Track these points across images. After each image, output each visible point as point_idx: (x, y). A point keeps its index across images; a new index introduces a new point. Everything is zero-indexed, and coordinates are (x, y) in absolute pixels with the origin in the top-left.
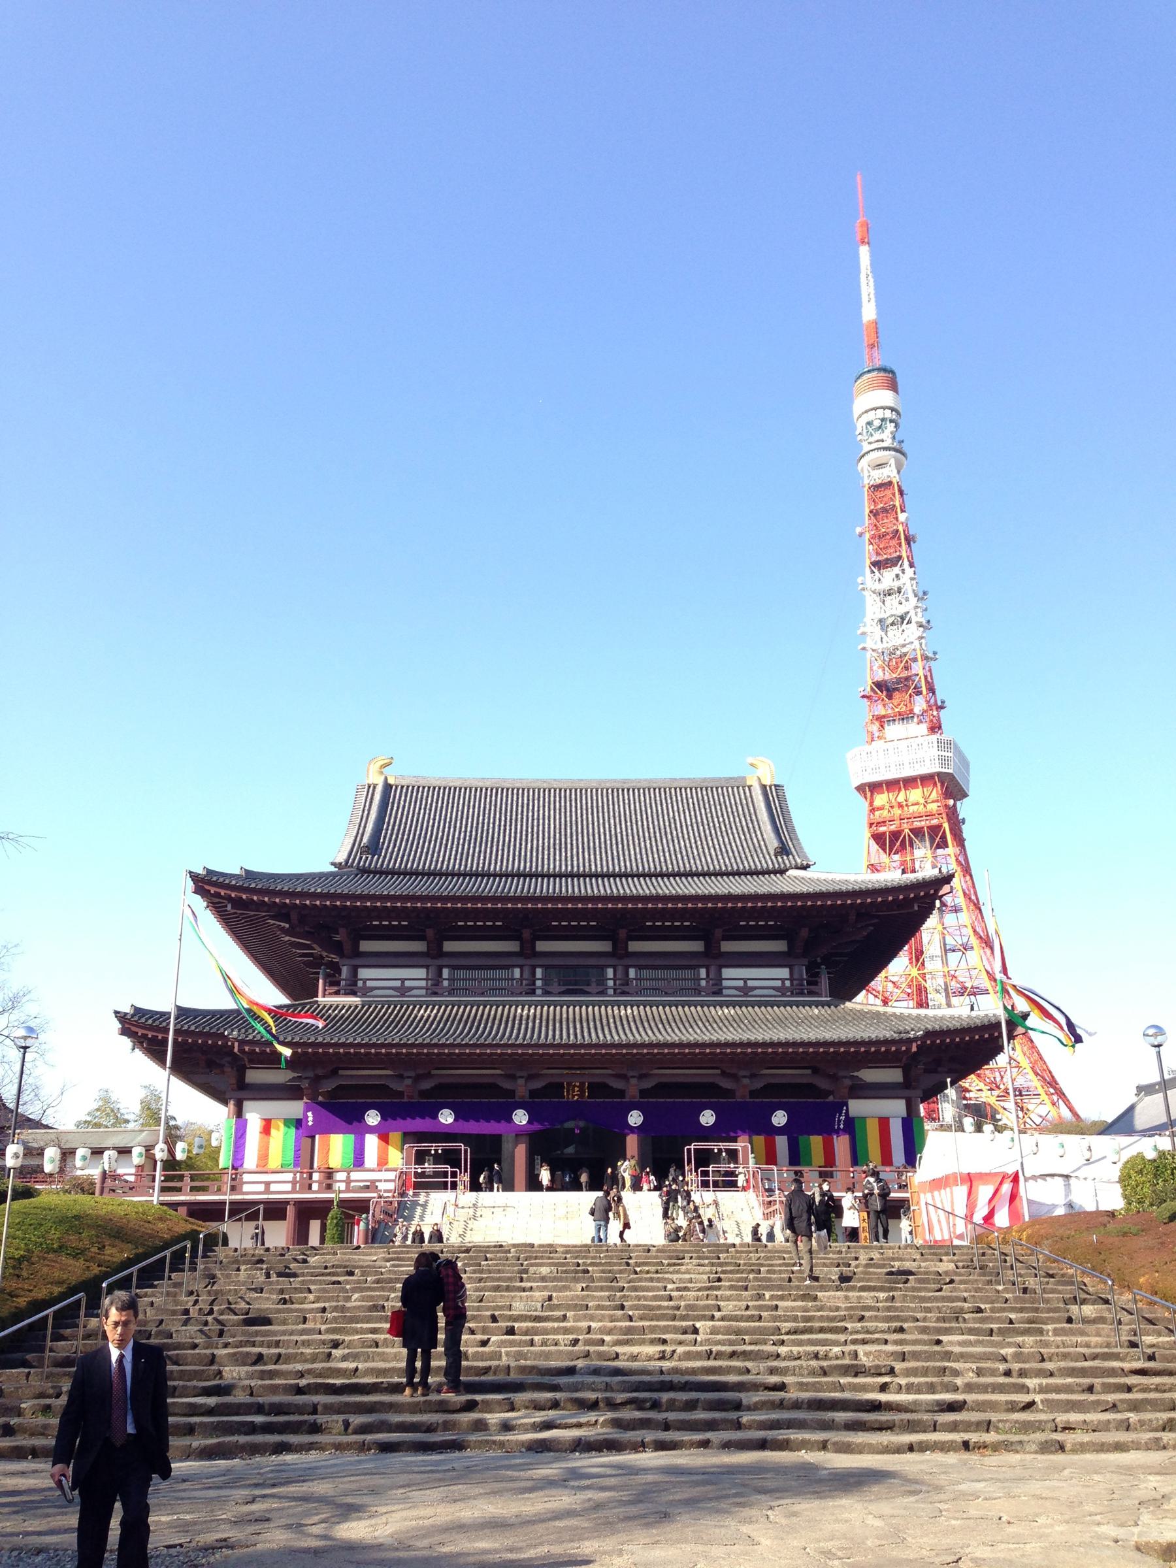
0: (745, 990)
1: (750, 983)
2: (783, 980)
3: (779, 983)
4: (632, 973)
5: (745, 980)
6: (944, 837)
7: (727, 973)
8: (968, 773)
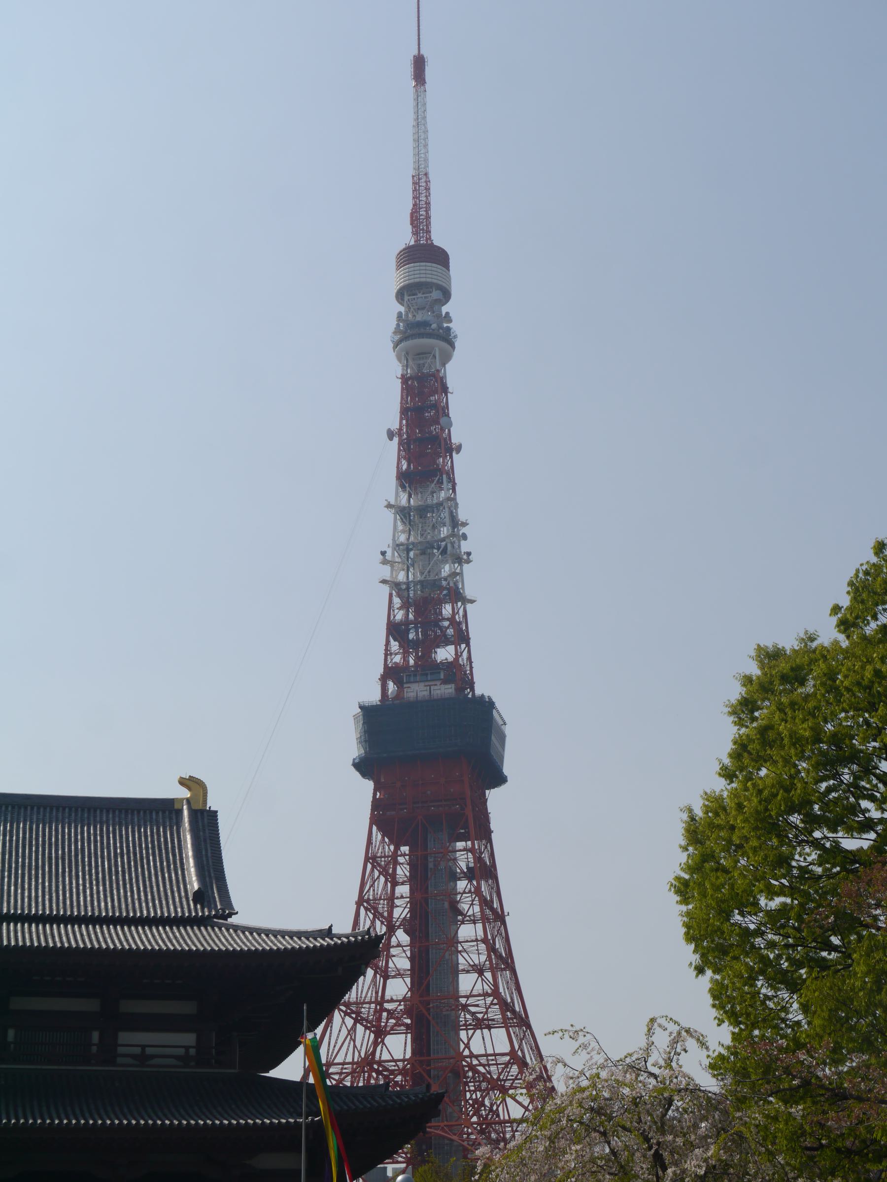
0: (143, 1058)
1: (149, 1051)
2: (187, 1048)
3: (181, 1051)
4: (11, 1033)
5: (143, 1047)
7: (125, 1037)
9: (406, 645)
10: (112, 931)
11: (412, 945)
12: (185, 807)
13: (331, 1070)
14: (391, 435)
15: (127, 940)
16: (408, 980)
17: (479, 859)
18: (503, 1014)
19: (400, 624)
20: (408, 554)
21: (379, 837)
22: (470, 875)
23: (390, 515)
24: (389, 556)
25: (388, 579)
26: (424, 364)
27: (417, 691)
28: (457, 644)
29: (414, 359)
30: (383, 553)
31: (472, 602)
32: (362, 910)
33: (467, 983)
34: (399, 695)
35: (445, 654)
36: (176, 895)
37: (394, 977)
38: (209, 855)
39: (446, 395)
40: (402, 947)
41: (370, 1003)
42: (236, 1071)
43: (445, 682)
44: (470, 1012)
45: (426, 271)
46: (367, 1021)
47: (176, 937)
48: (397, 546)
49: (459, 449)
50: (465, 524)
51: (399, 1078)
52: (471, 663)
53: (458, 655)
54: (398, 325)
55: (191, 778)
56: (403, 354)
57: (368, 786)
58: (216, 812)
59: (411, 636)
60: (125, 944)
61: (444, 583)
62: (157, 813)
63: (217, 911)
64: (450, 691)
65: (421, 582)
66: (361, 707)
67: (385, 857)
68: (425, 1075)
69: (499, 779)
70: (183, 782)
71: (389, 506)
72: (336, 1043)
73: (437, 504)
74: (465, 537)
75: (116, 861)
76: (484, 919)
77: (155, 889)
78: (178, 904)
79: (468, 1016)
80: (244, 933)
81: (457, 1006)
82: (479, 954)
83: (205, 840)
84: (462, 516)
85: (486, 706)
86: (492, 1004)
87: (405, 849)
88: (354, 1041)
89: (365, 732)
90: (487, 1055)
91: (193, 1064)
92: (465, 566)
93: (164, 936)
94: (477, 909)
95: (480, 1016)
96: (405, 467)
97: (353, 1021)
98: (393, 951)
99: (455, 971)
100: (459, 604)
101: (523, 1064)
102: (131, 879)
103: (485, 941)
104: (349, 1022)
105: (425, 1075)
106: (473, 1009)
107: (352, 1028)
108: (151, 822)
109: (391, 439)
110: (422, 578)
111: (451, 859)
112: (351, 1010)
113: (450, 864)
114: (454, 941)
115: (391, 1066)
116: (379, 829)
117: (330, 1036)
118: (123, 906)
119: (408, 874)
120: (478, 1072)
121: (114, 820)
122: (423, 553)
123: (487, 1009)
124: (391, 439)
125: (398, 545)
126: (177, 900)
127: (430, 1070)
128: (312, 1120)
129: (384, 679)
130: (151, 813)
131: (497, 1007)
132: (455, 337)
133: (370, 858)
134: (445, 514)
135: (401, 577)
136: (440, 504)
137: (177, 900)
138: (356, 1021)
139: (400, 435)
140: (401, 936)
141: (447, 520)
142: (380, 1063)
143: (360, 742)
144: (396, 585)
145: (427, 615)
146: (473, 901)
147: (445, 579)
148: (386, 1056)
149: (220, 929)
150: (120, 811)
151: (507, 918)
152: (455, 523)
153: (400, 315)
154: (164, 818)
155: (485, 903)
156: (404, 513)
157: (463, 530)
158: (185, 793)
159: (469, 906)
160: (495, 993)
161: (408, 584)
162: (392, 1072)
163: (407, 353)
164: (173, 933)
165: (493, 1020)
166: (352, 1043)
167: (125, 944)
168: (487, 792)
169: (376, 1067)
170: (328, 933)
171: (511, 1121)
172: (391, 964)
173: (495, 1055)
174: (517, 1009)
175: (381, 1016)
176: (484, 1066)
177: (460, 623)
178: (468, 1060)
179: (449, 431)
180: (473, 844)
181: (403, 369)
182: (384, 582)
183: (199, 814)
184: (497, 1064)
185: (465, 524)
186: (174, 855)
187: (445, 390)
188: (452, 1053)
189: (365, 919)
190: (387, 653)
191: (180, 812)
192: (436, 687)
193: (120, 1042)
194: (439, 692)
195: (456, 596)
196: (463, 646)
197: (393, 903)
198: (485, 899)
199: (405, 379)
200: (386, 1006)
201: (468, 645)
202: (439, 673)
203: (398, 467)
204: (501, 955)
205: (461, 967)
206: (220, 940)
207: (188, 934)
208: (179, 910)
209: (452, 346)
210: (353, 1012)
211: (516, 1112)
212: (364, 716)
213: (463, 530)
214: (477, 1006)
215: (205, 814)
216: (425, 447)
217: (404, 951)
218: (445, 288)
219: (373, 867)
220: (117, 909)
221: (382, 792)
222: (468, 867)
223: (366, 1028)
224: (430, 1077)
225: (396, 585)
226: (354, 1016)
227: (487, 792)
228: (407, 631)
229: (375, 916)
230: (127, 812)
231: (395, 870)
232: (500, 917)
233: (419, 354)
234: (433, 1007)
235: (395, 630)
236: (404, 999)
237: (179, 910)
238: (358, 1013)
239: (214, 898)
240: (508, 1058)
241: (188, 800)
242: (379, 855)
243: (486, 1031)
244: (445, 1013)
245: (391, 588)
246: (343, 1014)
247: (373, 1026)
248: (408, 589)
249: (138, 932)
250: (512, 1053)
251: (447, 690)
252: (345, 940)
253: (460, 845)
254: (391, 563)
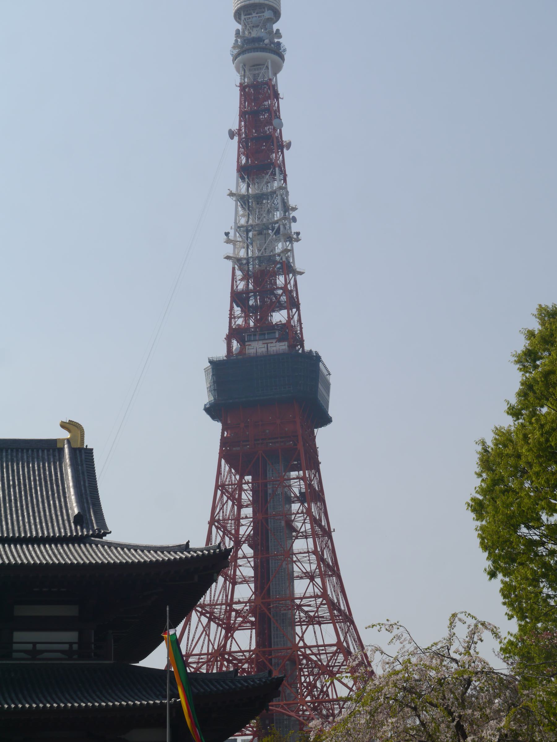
0: (34, 653)
1: (39, 647)
2: (71, 644)
3: (66, 647)
5: (35, 644)
6: (298, 459)
7: (18, 636)
8: (329, 396)
9: (247, 311)
10: (7, 549)
11: (255, 557)
12: (66, 446)
13: (190, 660)
14: (232, 135)
15: (20, 557)
16: (252, 586)
17: (309, 486)
18: (331, 612)
19: (242, 292)
20: (247, 234)
21: (227, 468)
22: (302, 498)
23: (231, 202)
24: (231, 236)
25: (231, 255)
26: (258, 74)
27: (257, 348)
28: (289, 309)
29: (250, 70)
30: (227, 234)
31: (301, 273)
32: (214, 529)
33: (301, 587)
34: (241, 352)
35: (279, 317)
36: (60, 518)
37: (241, 583)
38: (87, 485)
39: (278, 100)
40: (247, 558)
41: (221, 604)
42: (112, 662)
43: (280, 340)
44: (303, 611)
46: (219, 619)
47: (60, 553)
48: (238, 228)
49: (289, 145)
50: (294, 209)
51: (246, 666)
52: (301, 324)
53: (290, 318)
54: (236, 41)
55: (71, 422)
56: (241, 65)
57: (218, 426)
58: (92, 450)
59: (251, 302)
60: (18, 559)
61: (278, 258)
62: (43, 451)
63: (94, 531)
64: (284, 347)
65: (259, 258)
66: (211, 362)
67: (232, 485)
68: (267, 663)
69: (324, 419)
70: (64, 425)
71: (231, 194)
72: (194, 638)
73: (271, 192)
74: (294, 220)
75: (9, 491)
76: (314, 535)
77: (42, 514)
78: (61, 526)
79: (302, 614)
80: (116, 548)
81: (293, 606)
82: (310, 563)
83: (83, 473)
84: (292, 201)
85: (314, 360)
86: (321, 604)
87: (248, 478)
88: (209, 636)
89: (214, 382)
90: (318, 646)
91: (75, 657)
92: (295, 244)
93: (50, 552)
94: (308, 526)
95: (312, 614)
96: (244, 162)
97: (207, 620)
98: (240, 562)
99: (291, 578)
100: (291, 275)
101: (347, 653)
102: (22, 506)
103: (315, 552)
104: (204, 620)
105: (267, 663)
106: (306, 609)
107: (207, 625)
108: (38, 459)
109: (232, 137)
110: (260, 255)
111: (286, 486)
112: (205, 610)
113: (286, 489)
114: (290, 553)
115: (239, 656)
116: (227, 462)
117: (189, 632)
118: (16, 528)
119: (251, 499)
120: (311, 660)
121: (7, 457)
122: (260, 233)
123: (318, 608)
124: (232, 137)
125: (239, 227)
126: (61, 522)
127: (271, 659)
128: (175, 701)
129: (229, 339)
130: (38, 452)
131: (326, 606)
132: (285, 50)
133: (220, 486)
134: (278, 201)
135: (242, 253)
136: (274, 192)
137: (61, 522)
138: (210, 620)
139: (239, 135)
140: (246, 550)
141: (280, 206)
142: (230, 653)
143: (210, 391)
144: (237, 261)
145: (264, 284)
146: (305, 520)
147: (279, 255)
148: (235, 648)
149: (97, 546)
150: (12, 450)
151: (333, 534)
152: (286, 208)
153: (238, 32)
154: (48, 455)
155: (315, 522)
156: (244, 200)
157: (293, 214)
158: (65, 435)
159: (302, 524)
160: (324, 595)
161: (248, 259)
162: (240, 661)
163: (245, 65)
164: (58, 550)
165: (323, 617)
166: (207, 637)
167: (18, 559)
168: (316, 430)
169: (226, 657)
170: (186, 547)
171: (338, 700)
172: (238, 573)
173: (324, 646)
174: (342, 608)
175: (230, 615)
176: (315, 655)
177: (291, 291)
178: (303, 650)
179: (281, 131)
180: (304, 473)
181: (241, 79)
182: (228, 258)
183: (78, 452)
184: (326, 653)
185: (294, 209)
186: (58, 486)
187: (276, 96)
188: (289, 645)
189: (216, 536)
190: (232, 317)
191: (62, 450)
192: (272, 345)
193: (15, 640)
194: (274, 348)
195: (288, 268)
196: (294, 310)
197: (239, 522)
198: (315, 518)
199: (243, 87)
200: (235, 607)
201: (298, 309)
202: (275, 332)
203: (238, 162)
204: (328, 564)
205: (295, 574)
206: (96, 555)
207: (70, 550)
208: (62, 531)
209: (282, 58)
210: (207, 612)
211: (343, 692)
212: (213, 369)
213: (293, 214)
214: (309, 606)
215: (83, 451)
216: (260, 145)
217: (249, 562)
218: (276, 9)
219: (222, 493)
220: (10, 531)
221: (229, 431)
222: (300, 492)
223: (218, 625)
224: (271, 664)
225: (237, 261)
226: (208, 615)
227: (316, 430)
228: (248, 299)
229: (224, 534)
230: (17, 450)
231: (240, 495)
232: (327, 533)
233: (254, 66)
234: (273, 607)
235: (238, 298)
236: (250, 601)
237: (62, 531)
238: (212, 613)
239: (92, 520)
240: (335, 648)
241: (68, 440)
242: (227, 483)
243: (317, 626)
244: (282, 612)
245: (234, 263)
246: (199, 614)
247: (224, 623)
248: (248, 263)
249: (28, 550)
250: (339, 644)
251: (282, 347)
252: (200, 553)
253: (294, 474)
254: (234, 242)
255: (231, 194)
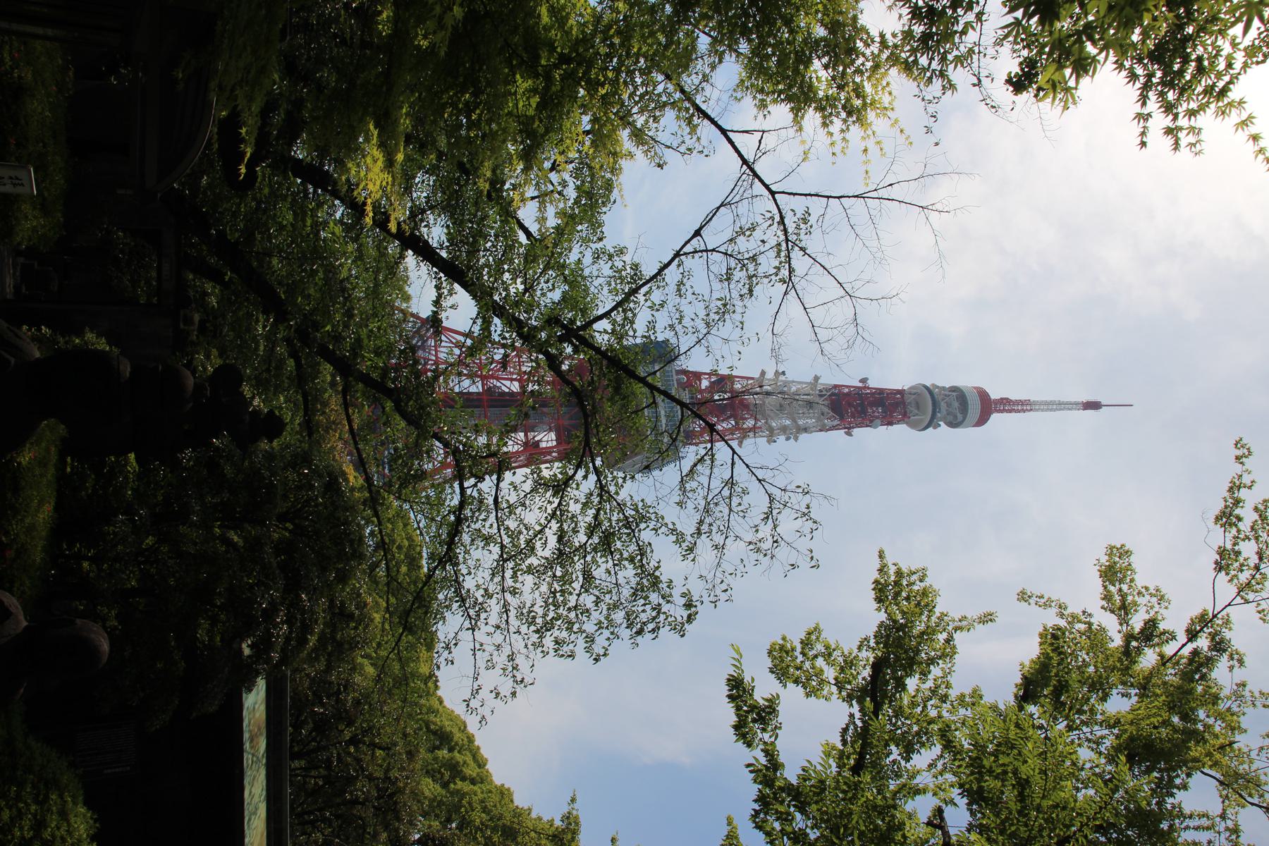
14: (864, 381)
23: (809, 379)
24: (782, 378)
30: (783, 373)
45: (975, 408)
48: (786, 383)
49: (849, 434)
74: (788, 439)
182: (763, 373)
185: (796, 439)
255: (816, 378)
